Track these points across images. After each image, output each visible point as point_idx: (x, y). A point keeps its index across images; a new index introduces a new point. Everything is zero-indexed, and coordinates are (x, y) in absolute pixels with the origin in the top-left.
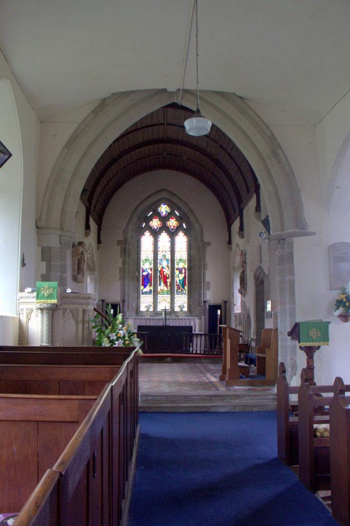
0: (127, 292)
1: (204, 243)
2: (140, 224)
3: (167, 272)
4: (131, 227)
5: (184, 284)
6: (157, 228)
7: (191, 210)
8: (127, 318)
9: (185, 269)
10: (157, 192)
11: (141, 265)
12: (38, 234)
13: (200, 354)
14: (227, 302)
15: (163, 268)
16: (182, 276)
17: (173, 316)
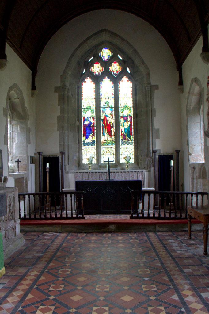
0: (66, 142)
1: (151, 86)
2: (81, 71)
3: (111, 120)
5: (130, 134)
6: (99, 73)
7: (135, 51)
8: (67, 173)
9: (131, 117)
10: (98, 33)
13: (154, 218)
14: (179, 151)
15: (106, 116)
16: (127, 125)
17: (118, 169)
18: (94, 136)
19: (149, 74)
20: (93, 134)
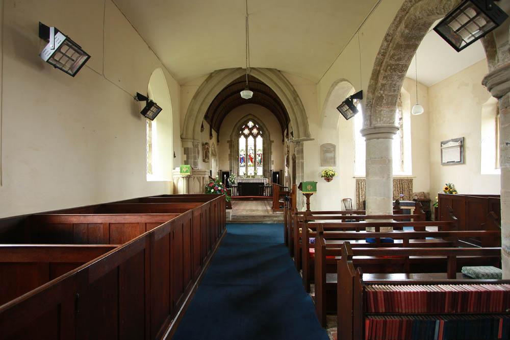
2: (239, 132)
3: (253, 156)
4: (234, 134)
7: (264, 124)
10: (247, 116)
12: (182, 141)
19: (270, 136)
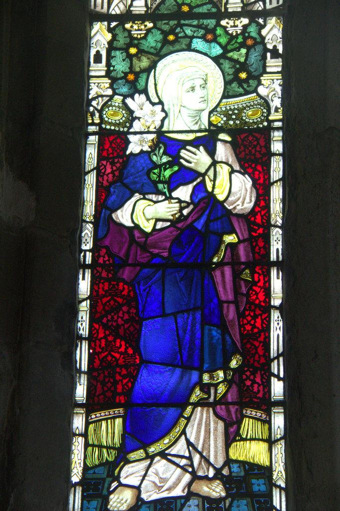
11: (99, 87)
18: (266, 404)
20: (235, 380)
